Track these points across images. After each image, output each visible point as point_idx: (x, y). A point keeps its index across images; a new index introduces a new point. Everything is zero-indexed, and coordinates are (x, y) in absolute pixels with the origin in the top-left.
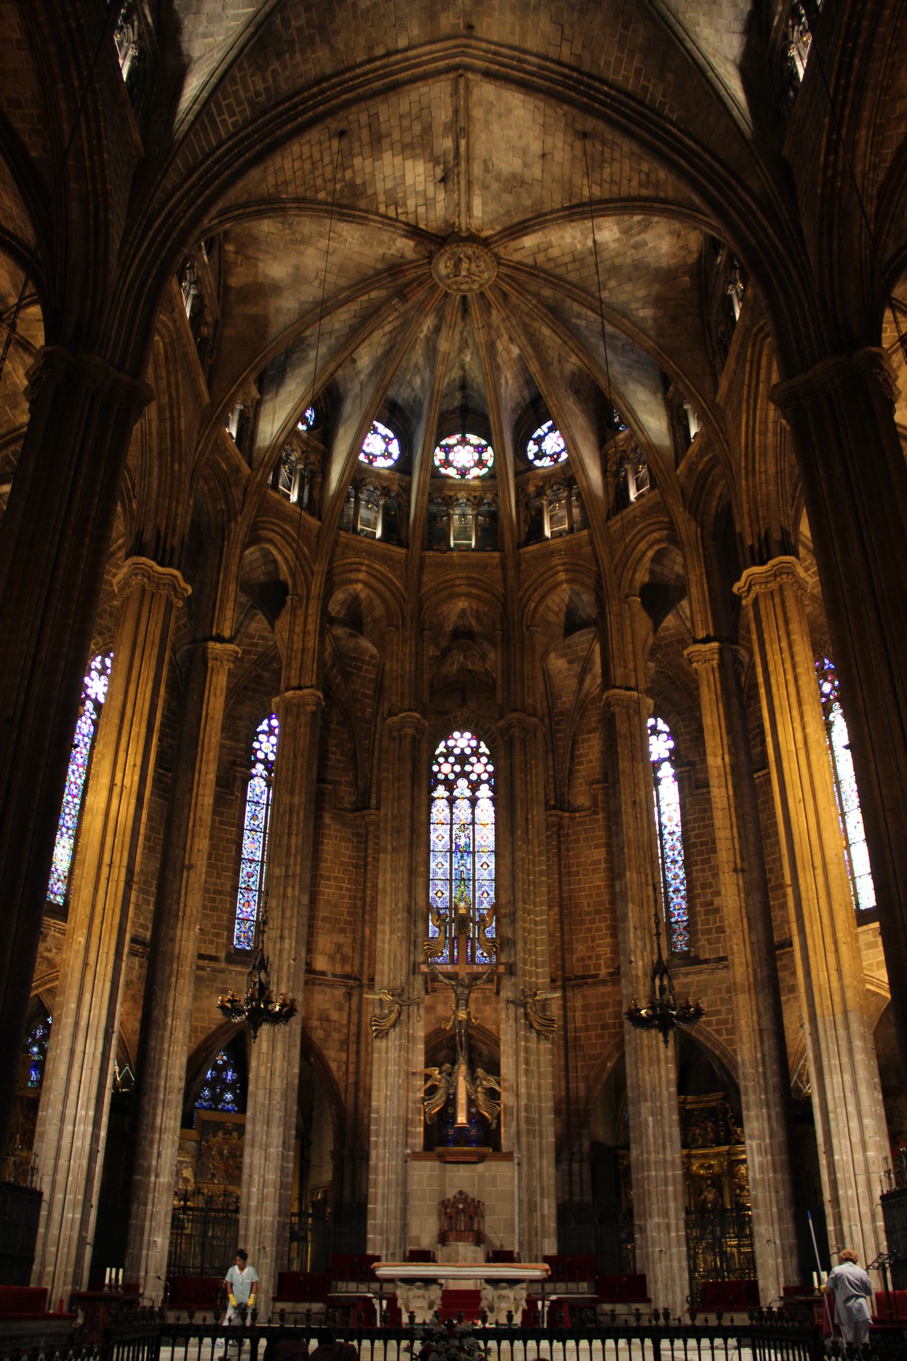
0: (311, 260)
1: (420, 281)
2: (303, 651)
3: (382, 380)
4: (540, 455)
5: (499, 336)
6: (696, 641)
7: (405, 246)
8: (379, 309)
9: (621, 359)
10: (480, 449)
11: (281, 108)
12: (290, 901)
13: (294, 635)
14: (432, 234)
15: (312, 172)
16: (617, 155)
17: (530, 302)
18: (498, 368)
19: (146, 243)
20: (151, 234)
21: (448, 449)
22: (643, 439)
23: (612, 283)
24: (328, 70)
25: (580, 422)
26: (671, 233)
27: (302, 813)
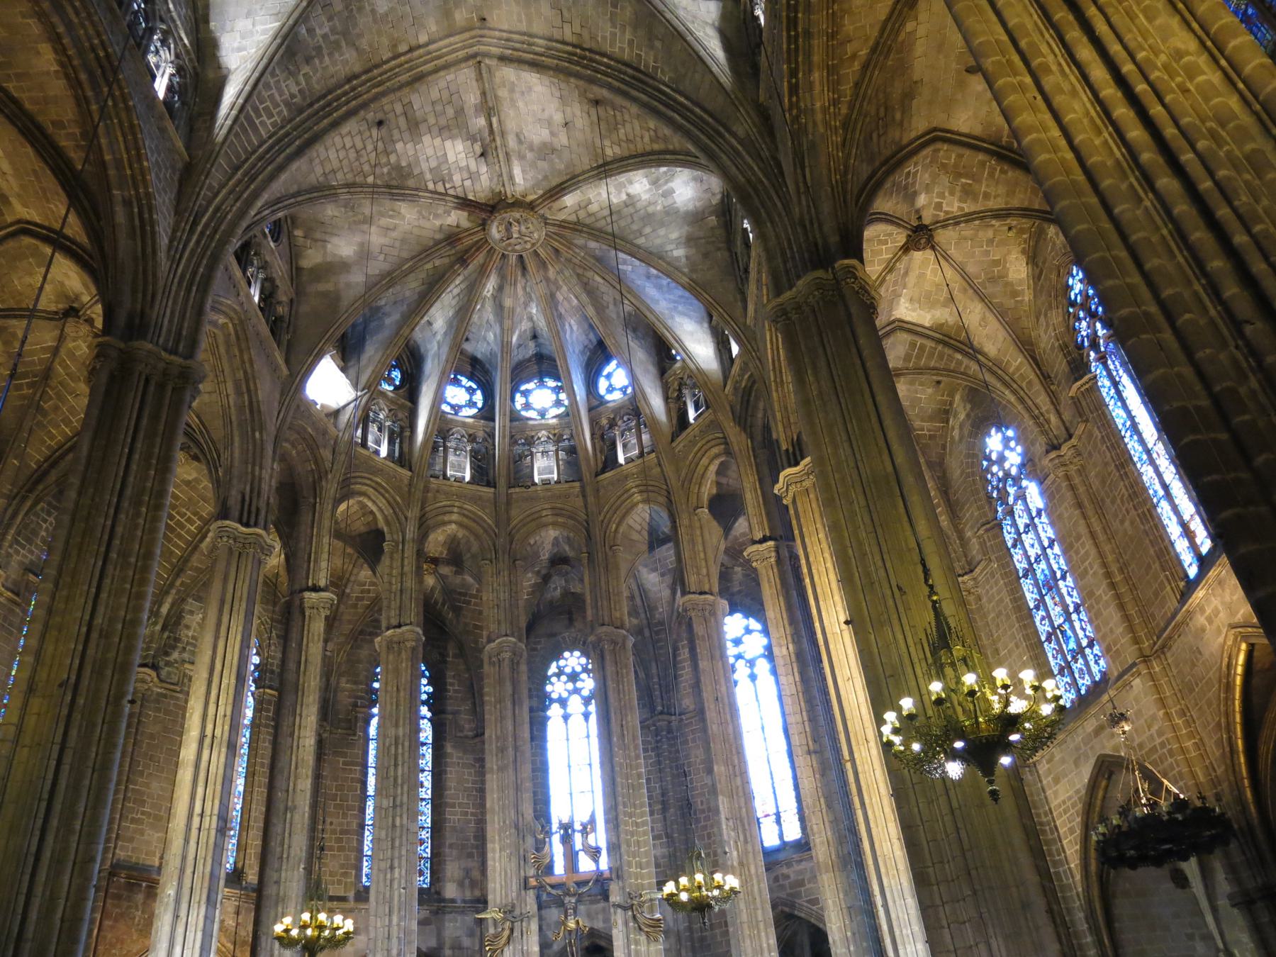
1: (478, 246)
2: (401, 591)
3: (455, 338)
4: (611, 389)
5: (559, 288)
6: (754, 542)
7: (456, 218)
8: (443, 275)
9: (667, 296)
10: (557, 390)
11: (316, 106)
12: (398, 830)
13: (393, 580)
15: (357, 159)
16: (627, 117)
18: (560, 316)
19: (195, 238)
20: (199, 228)
21: (526, 394)
22: (692, 366)
23: (648, 230)
24: (357, 68)
25: (641, 355)
26: (695, 179)
27: (407, 744)
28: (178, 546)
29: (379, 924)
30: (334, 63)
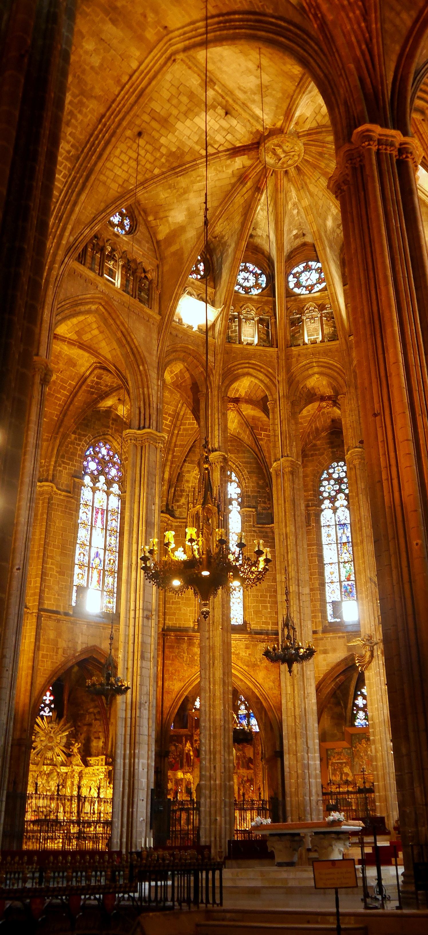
14: (249, 145)
24: (102, 110)
30: (86, 116)
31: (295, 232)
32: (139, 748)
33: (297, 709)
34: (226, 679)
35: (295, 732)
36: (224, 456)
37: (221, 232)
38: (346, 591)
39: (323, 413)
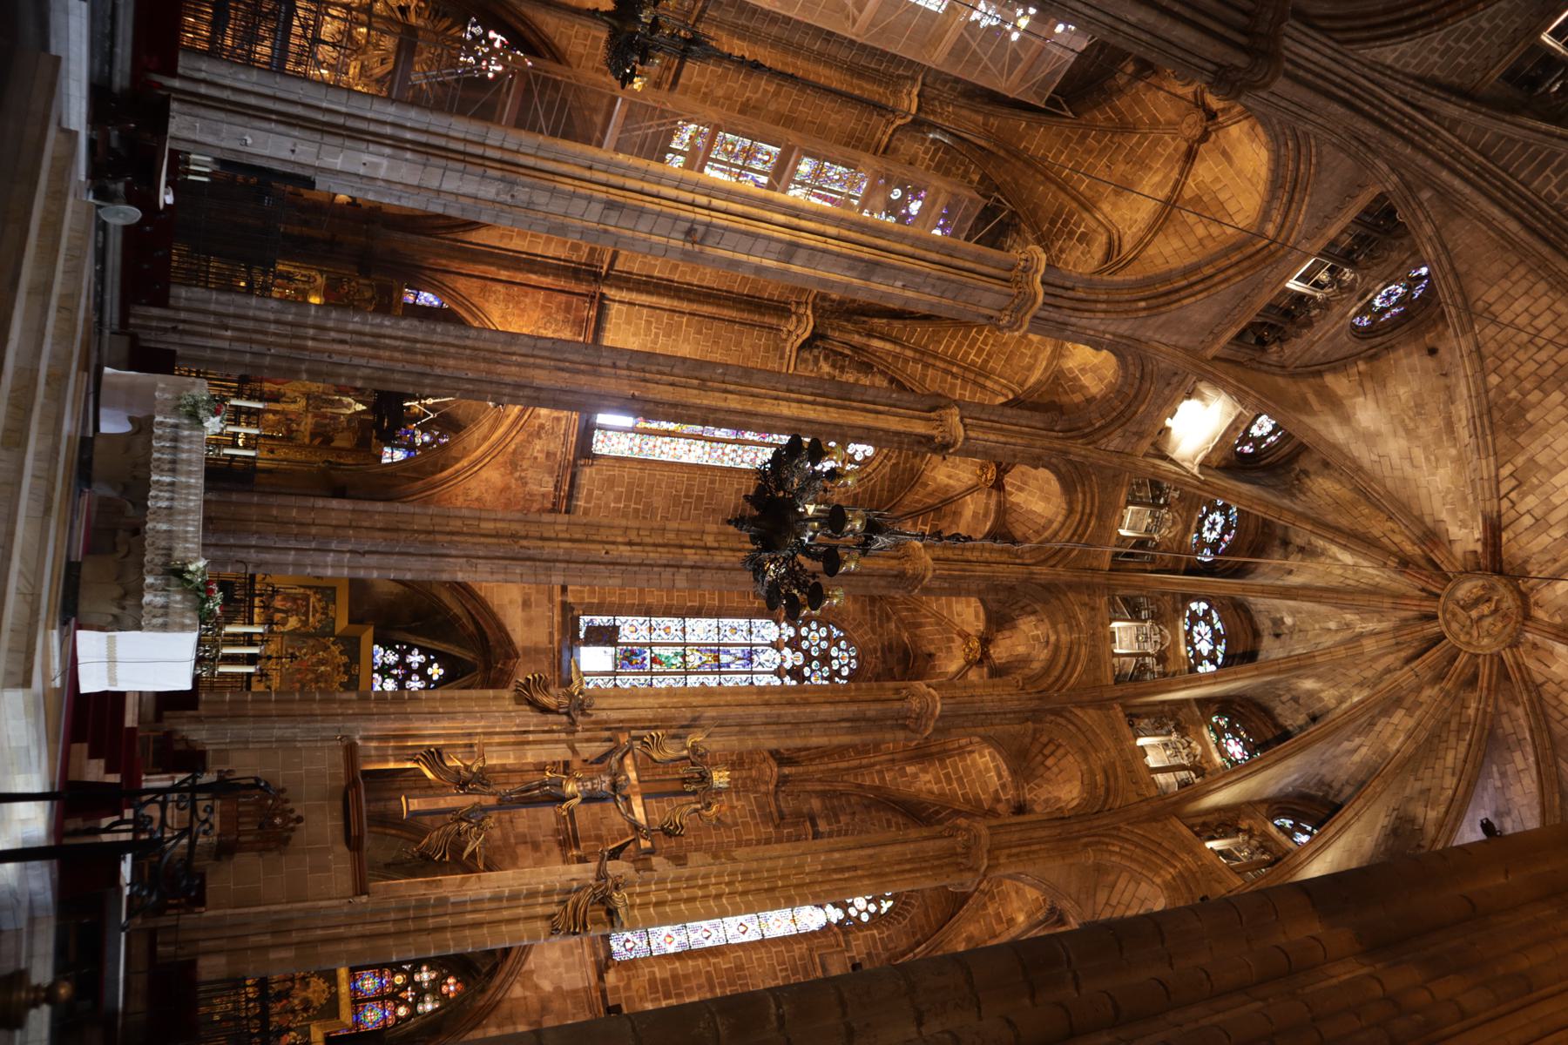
0: (1394, 447)
5: (1410, 712)
17: (1487, 705)
28: (948, 347)
29: (558, 528)
31: (1289, 621)
32: (414, 162)
33: (448, 538)
34: (528, 392)
35: (397, 530)
36: (953, 445)
37: (1310, 489)
38: (633, 653)
39: (952, 640)
